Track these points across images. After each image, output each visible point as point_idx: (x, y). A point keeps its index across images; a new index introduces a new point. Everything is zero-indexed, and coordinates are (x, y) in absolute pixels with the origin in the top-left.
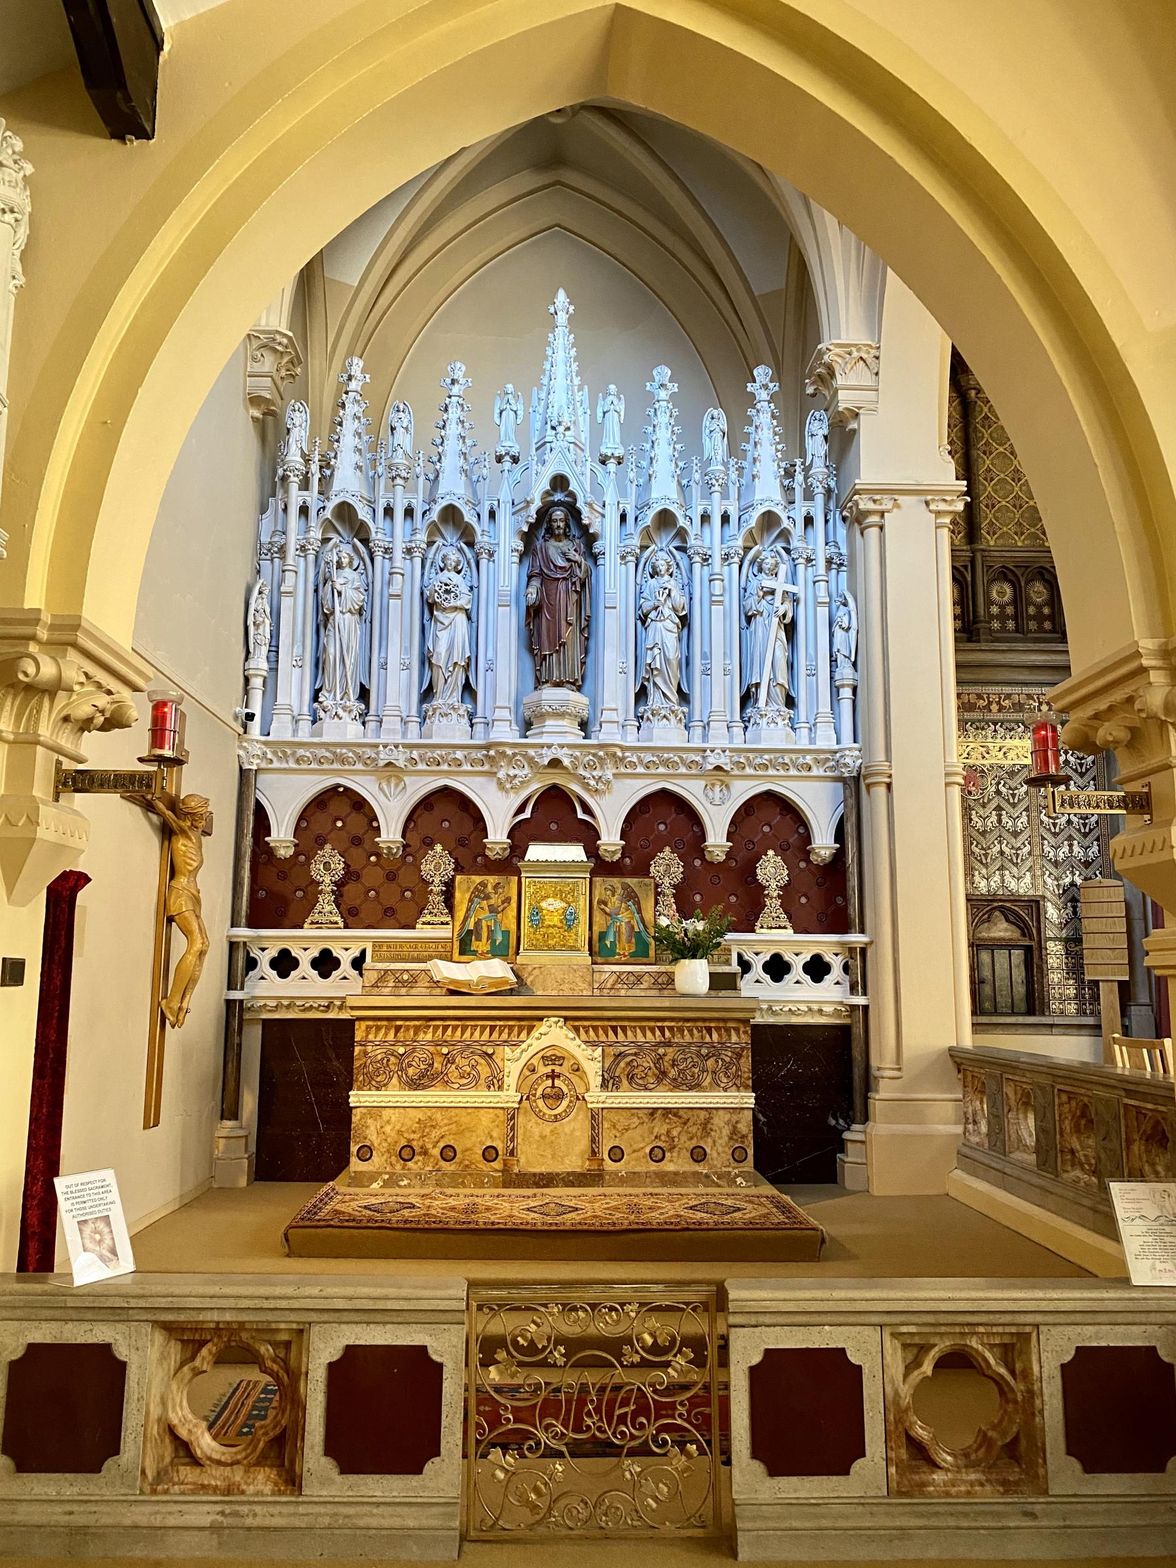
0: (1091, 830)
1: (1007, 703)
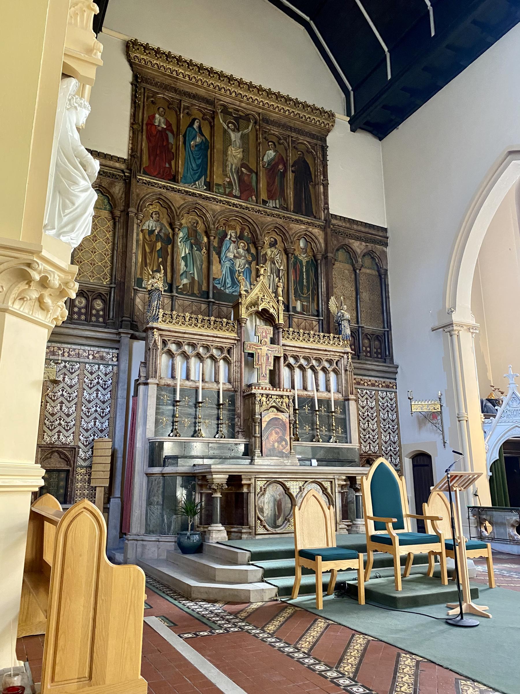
0: (106, 415)
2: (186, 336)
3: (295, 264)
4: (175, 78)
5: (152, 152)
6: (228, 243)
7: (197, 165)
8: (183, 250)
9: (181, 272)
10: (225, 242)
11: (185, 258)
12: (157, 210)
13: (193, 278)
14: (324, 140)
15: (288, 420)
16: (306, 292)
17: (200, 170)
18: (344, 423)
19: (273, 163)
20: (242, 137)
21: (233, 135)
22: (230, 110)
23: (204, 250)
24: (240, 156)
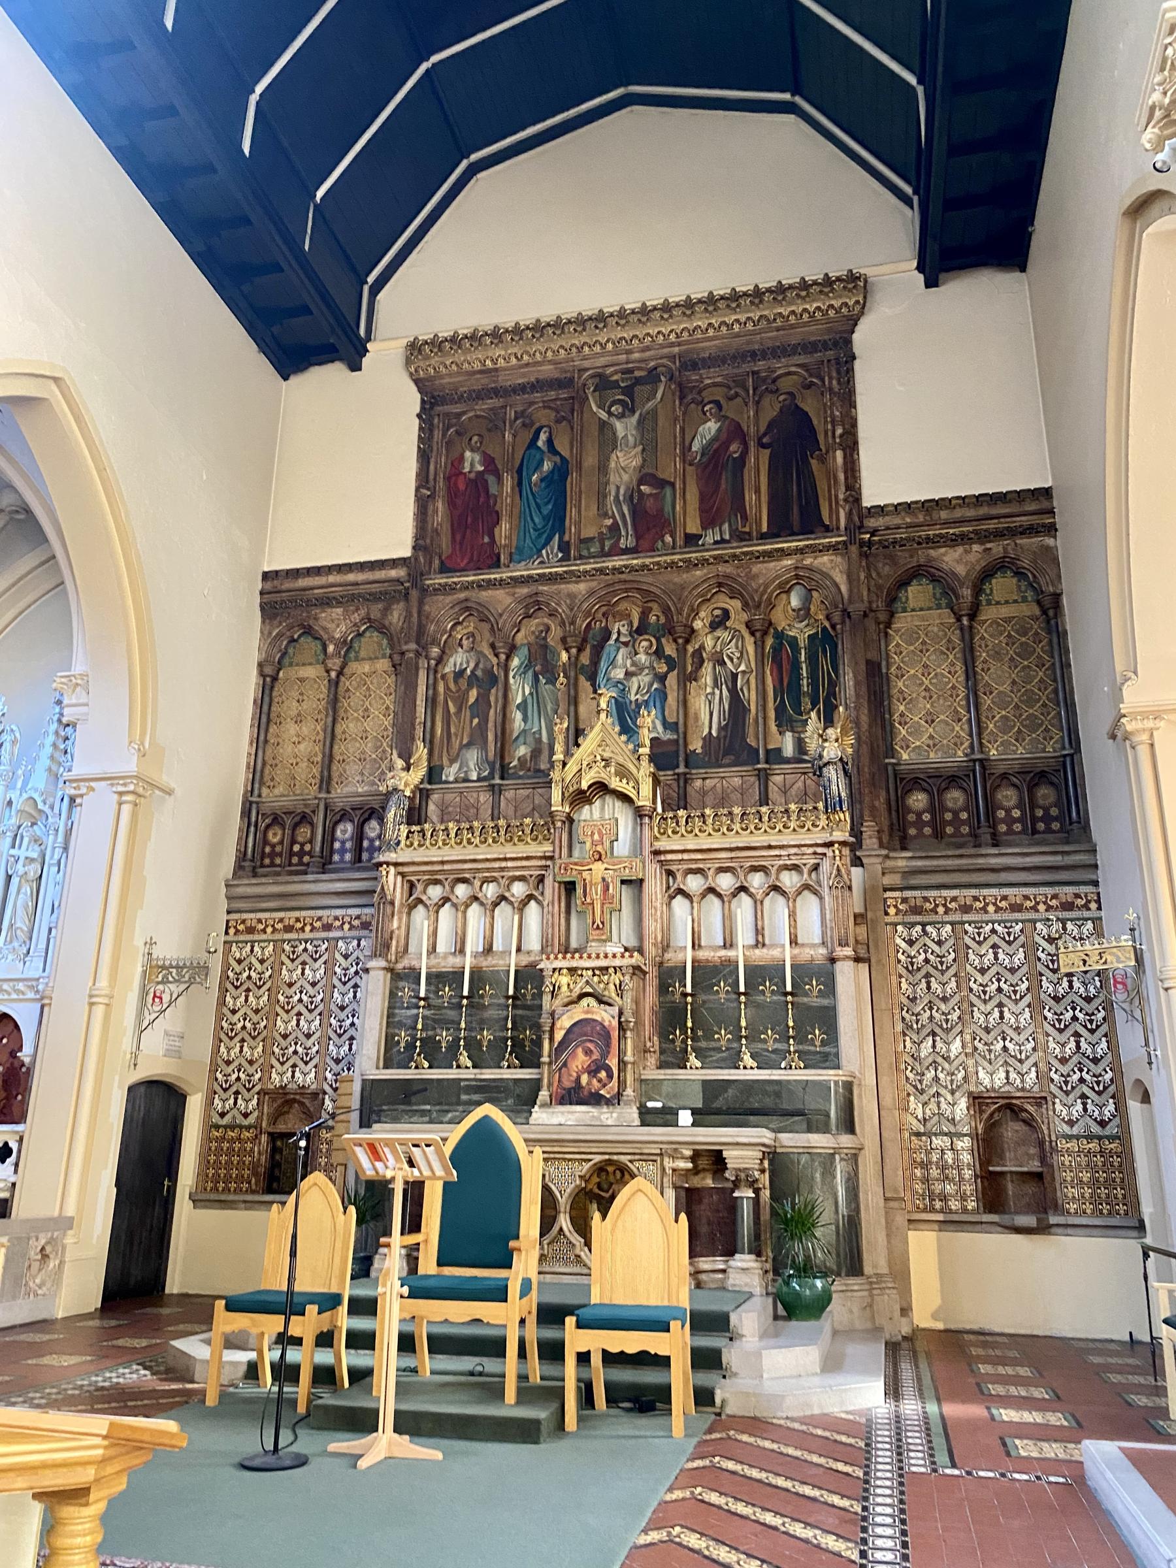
2: (446, 867)
3: (777, 650)
7: (544, 518)
8: (520, 689)
9: (515, 735)
10: (606, 650)
11: (523, 707)
12: (471, 629)
14: (848, 342)
15: (615, 1023)
16: (809, 706)
20: (641, 422)
21: (619, 426)
22: (615, 378)
23: (562, 679)
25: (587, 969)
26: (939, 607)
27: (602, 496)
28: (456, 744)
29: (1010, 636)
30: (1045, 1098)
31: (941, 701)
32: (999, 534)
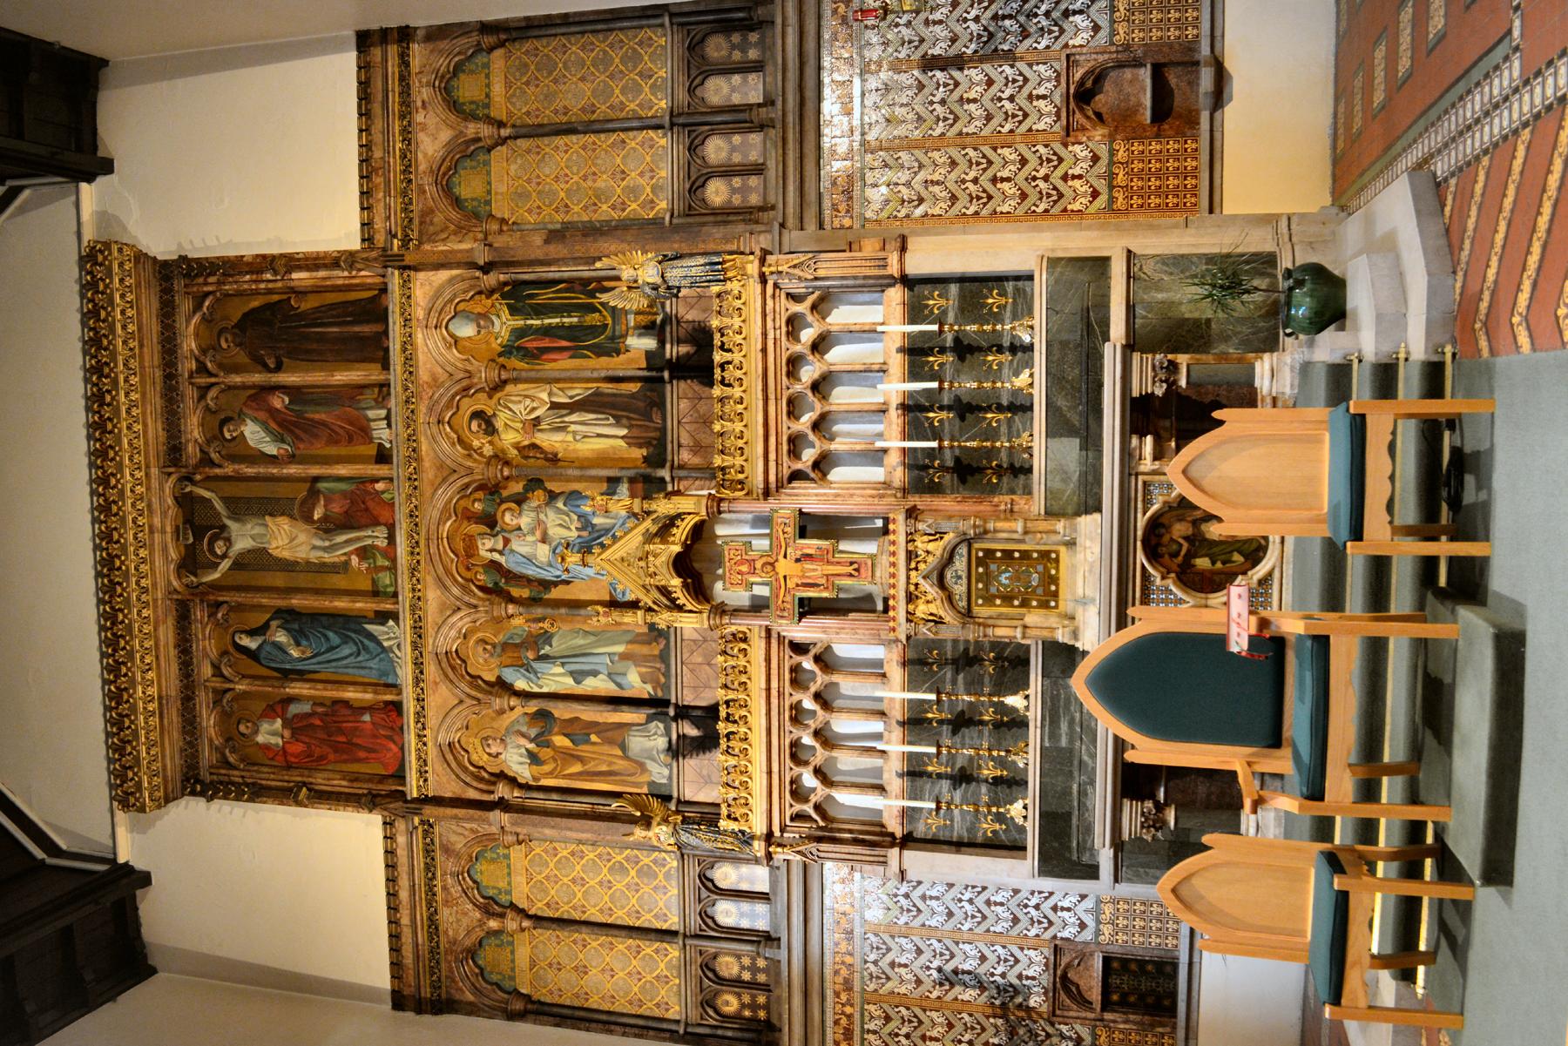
1: (844, 997)
4: (160, 704)
5: (347, 750)
6: (512, 558)
8: (556, 679)
11: (578, 676)
12: (477, 742)
13: (624, 657)
14: (165, 264)
16: (597, 315)
17: (353, 635)
18: (975, 287)
19: (273, 425)
20: (237, 516)
23: (546, 625)
24: (284, 523)
25: (908, 578)
26: (487, 163)
27: (322, 568)
28: (621, 765)
29: (527, 83)
30: (1068, 56)
31: (599, 162)
32: (406, 91)
